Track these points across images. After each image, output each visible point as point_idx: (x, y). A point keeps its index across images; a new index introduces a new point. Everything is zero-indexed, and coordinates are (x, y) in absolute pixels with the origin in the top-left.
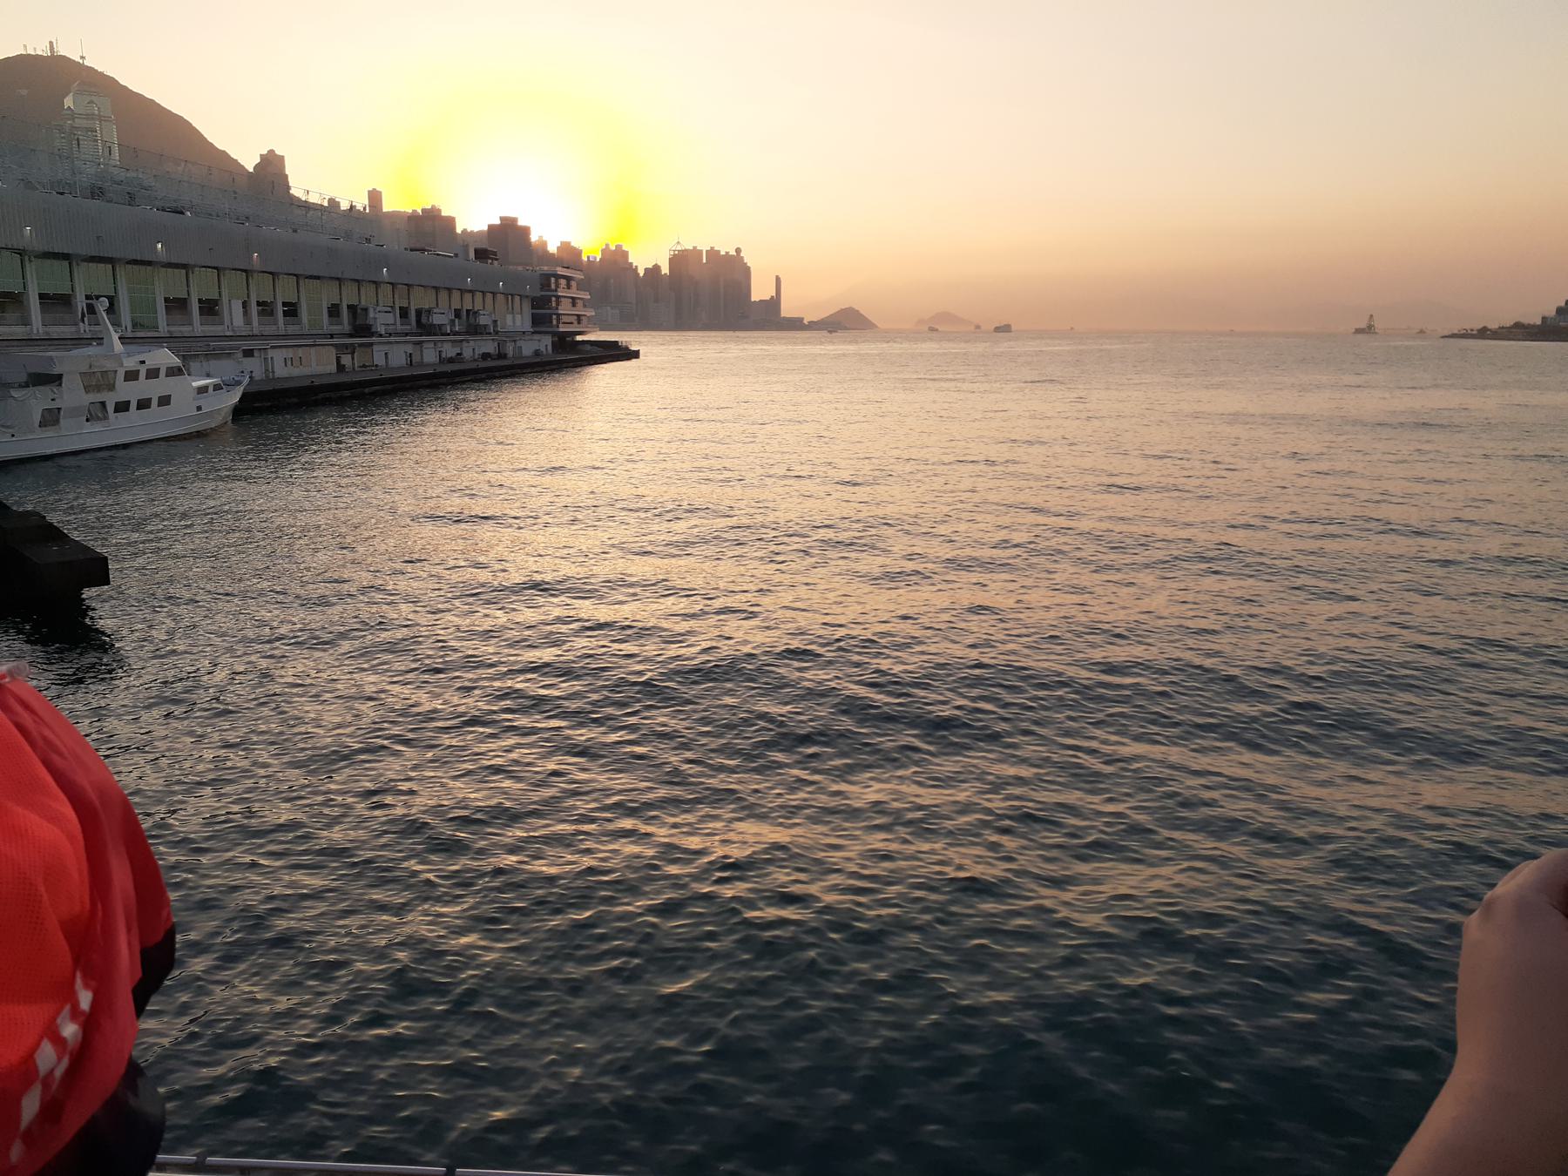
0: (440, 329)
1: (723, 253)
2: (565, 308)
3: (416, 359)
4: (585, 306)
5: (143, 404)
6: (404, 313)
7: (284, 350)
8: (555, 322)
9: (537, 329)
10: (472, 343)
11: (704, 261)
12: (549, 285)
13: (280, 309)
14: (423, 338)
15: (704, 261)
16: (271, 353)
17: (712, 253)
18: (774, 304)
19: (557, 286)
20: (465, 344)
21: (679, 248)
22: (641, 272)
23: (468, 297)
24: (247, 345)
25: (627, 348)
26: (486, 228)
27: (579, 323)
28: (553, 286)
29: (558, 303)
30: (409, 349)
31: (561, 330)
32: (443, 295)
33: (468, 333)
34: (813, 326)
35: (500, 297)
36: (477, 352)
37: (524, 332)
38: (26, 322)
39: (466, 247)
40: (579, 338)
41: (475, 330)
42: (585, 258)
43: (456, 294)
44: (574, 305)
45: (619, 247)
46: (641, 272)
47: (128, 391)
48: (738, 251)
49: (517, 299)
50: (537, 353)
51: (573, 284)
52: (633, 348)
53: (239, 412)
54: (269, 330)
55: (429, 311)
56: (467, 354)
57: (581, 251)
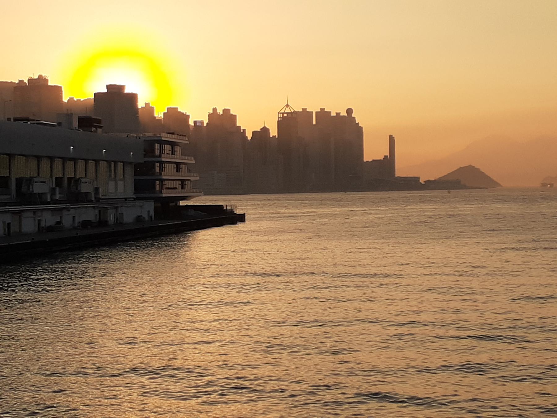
1: (333, 114)
2: (169, 173)
3: (14, 228)
4: (189, 171)
8: (158, 188)
9: (139, 195)
10: (72, 211)
11: (314, 123)
12: (153, 150)
15: (314, 123)
17: (323, 114)
19: (161, 151)
20: (65, 212)
21: (288, 110)
22: (249, 136)
23: (70, 164)
25: (232, 212)
26: (92, 97)
27: (183, 188)
28: (157, 152)
29: (161, 169)
30: (8, 218)
31: (164, 195)
32: (45, 165)
35: (103, 165)
36: (77, 220)
37: (126, 199)
39: (69, 115)
40: (182, 203)
42: (191, 123)
43: (58, 163)
44: (178, 170)
45: (226, 111)
46: (249, 136)
48: (349, 111)
49: (120, 165)
50: (139, 219)
51: (178, 148)
52: (238, 212)
55: (30, 181)
56: (67, 222)
57: (188, 116)
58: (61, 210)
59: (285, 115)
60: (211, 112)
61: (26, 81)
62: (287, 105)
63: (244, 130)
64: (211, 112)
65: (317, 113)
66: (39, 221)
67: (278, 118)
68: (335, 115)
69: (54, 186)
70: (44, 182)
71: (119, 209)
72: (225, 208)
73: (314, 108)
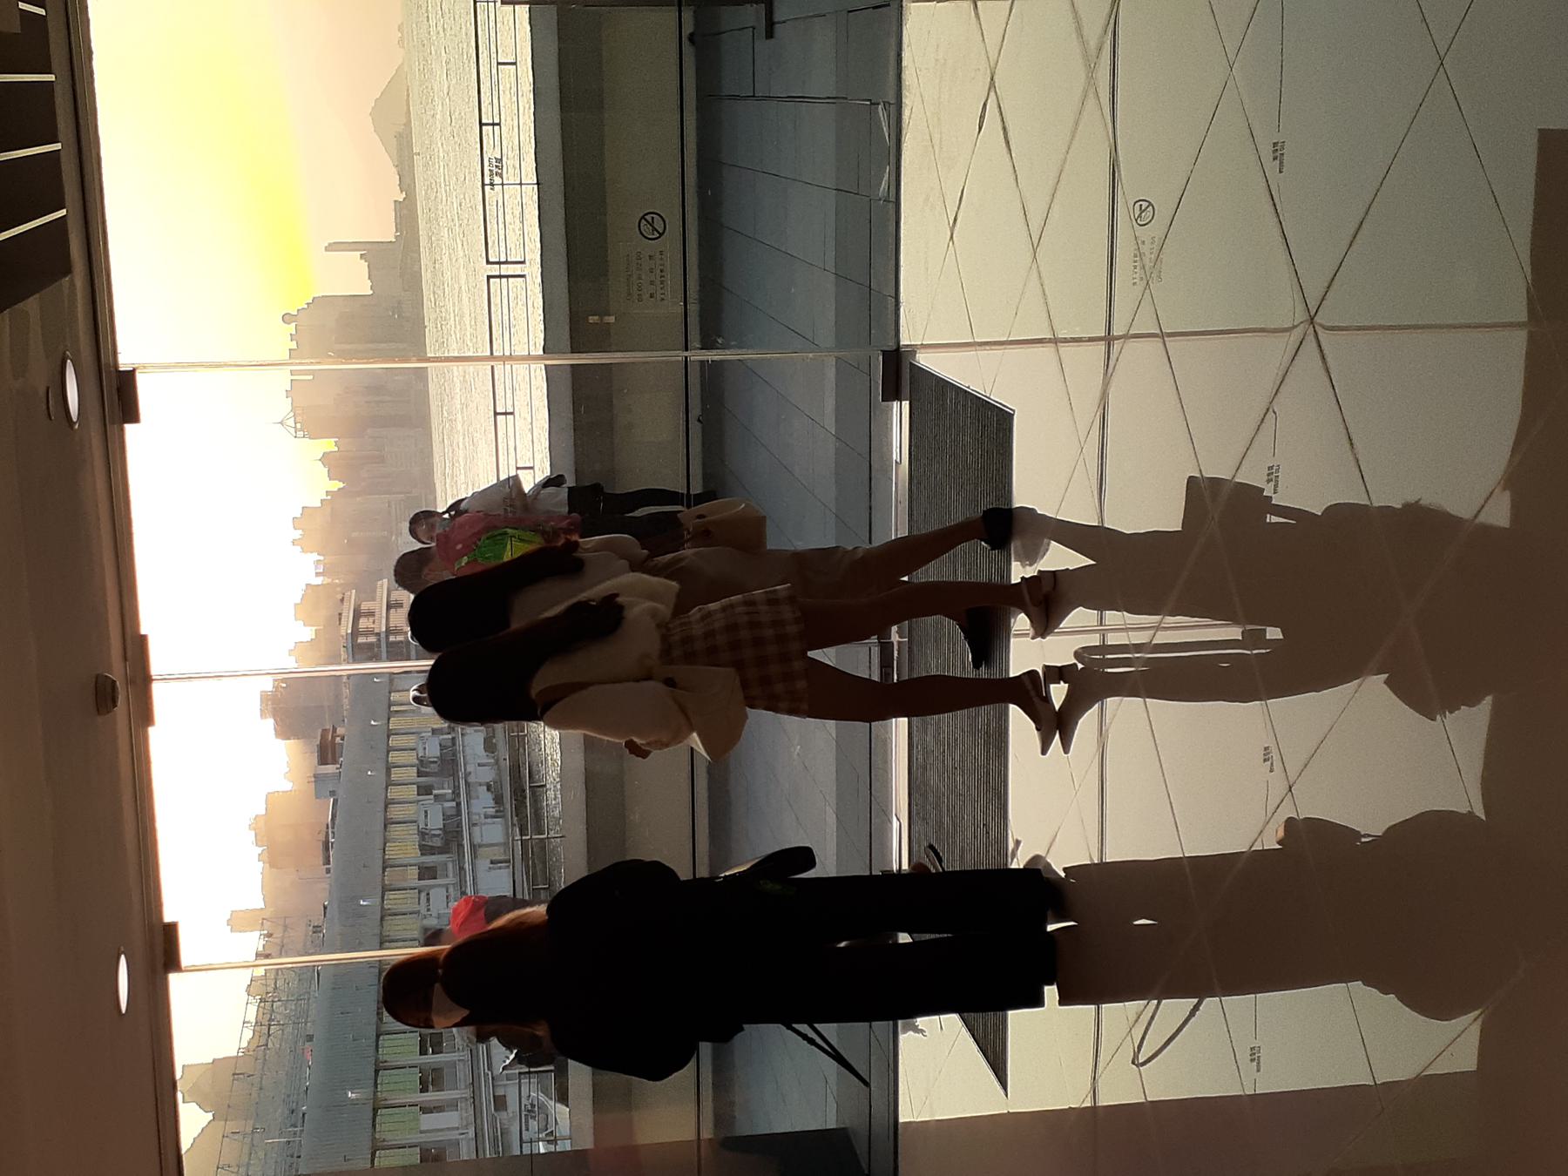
0: (449, 817)
6: (427, 872)
14: (466, 842)
18: (372, 253)
20: (471, 779)
21: (291, 422)
22: (337, 485)
32: (396, 812)
33: (454, 775)
34: (406, 181)
35: (395, 723)
42: (319, 581)
43: (394, 793)
46: (337, 485)
48: (287, 318)
54: (463, 1073)
55: (423, 834)
56: (487, 775)
58: (467, 784)
59: (299, 426)
61: (259, 850)
66: (486, 817)
67: (304, 437)
69: (432, 797)
70: (426, 812)
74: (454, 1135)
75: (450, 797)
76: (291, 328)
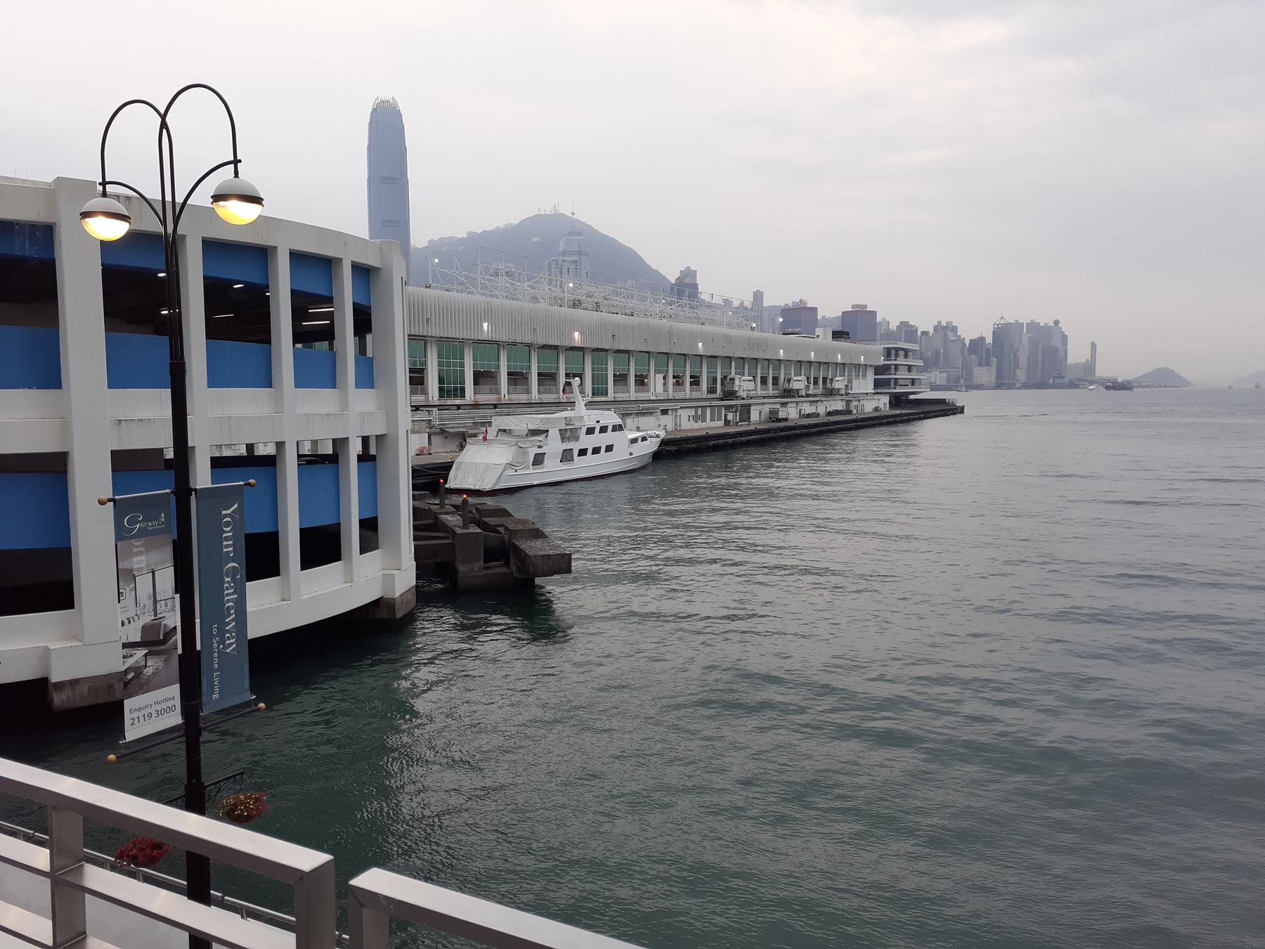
5: (596, 451)
7: (689, 410)
9: (879, 391)
13: (688, 380)
14: (789, 400)
16: (680, 412)
18: (1090, 366)
21: (1002, 322)
22: (967, 342)
24: (664, 406)
25: (953, 404)
26: (841, 314)
27: (913, 385)
37: (867, 394)
38: (528, 391)
40: (912, 397)
41: (831, 393)
46: (967, 342)
47: (587, 442)
48: (1057, 323)
50: (876, 409)
51: (910, 354)
53: (657, 456)
54: (680, 395)
58: (817, 401)
60: (936, 324)
62: (1002, 318)
63: (964, 339)
64: (936, 324)
65: (1027, 323)
66: (800, 410)
68: (1043, 325)
71: (861, 402)
72: (947, 401)
73: (1025, 320)
74: (652, 390)
75: (808, 392)
76: (1051, 324)
